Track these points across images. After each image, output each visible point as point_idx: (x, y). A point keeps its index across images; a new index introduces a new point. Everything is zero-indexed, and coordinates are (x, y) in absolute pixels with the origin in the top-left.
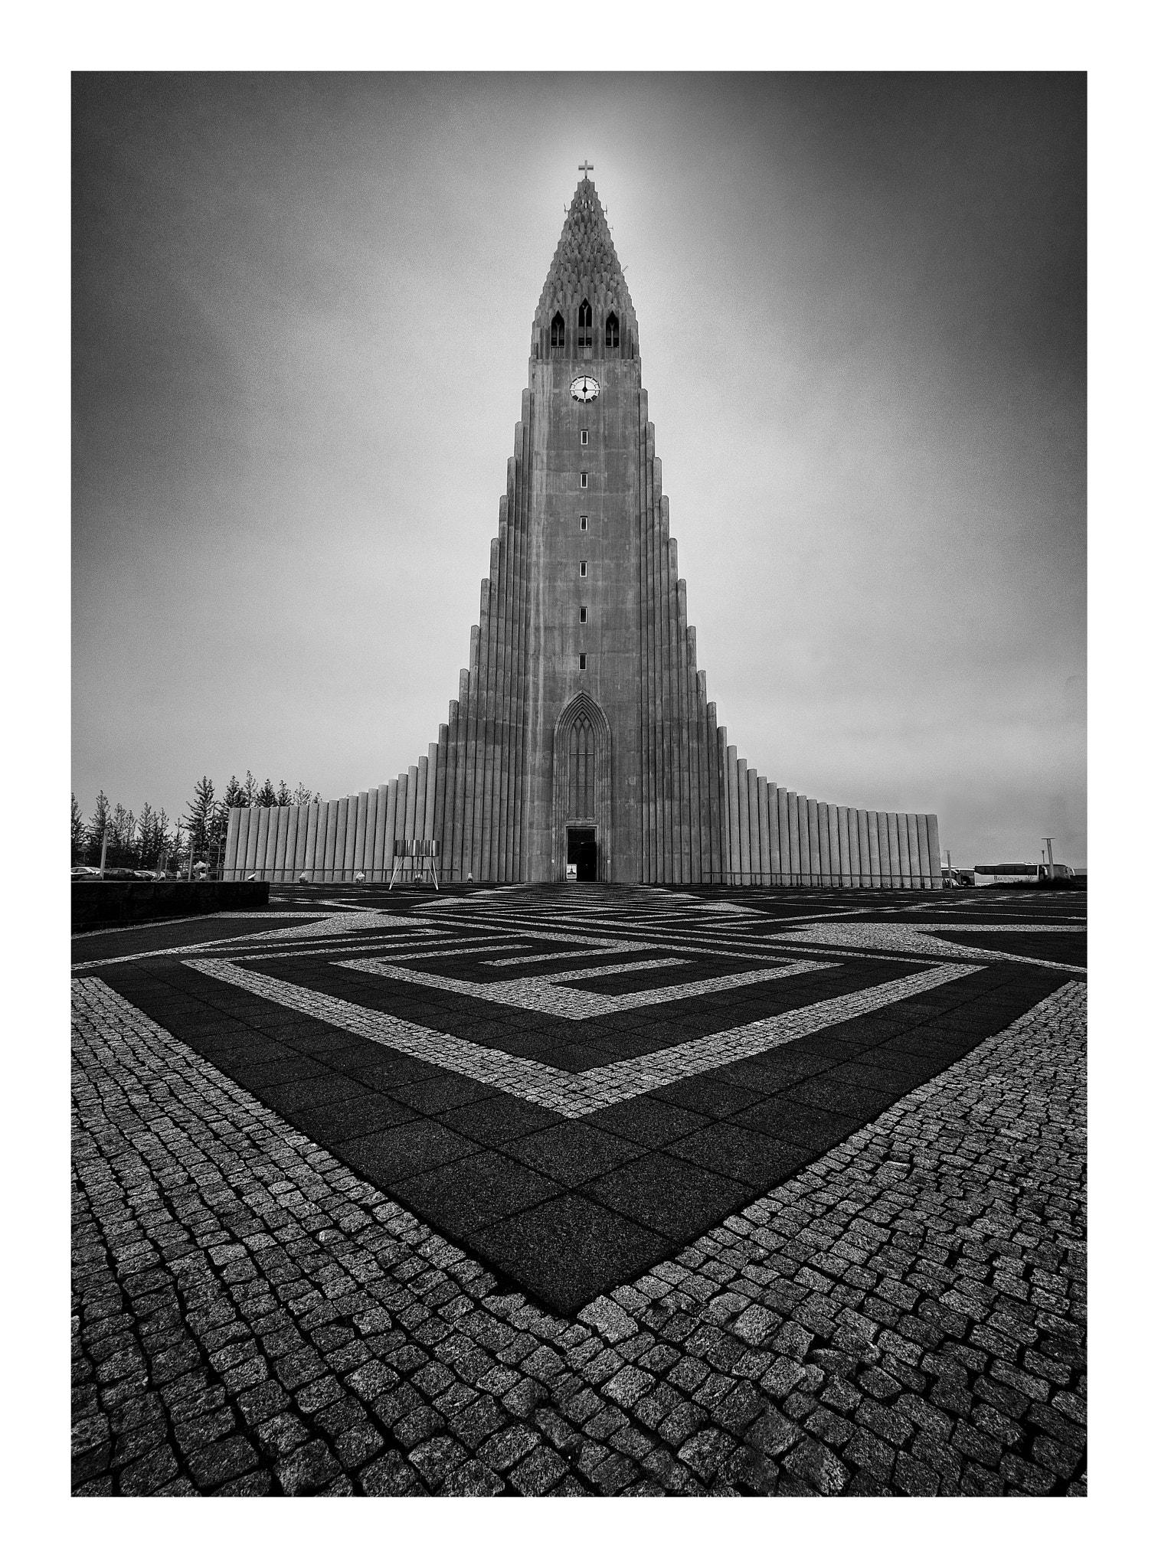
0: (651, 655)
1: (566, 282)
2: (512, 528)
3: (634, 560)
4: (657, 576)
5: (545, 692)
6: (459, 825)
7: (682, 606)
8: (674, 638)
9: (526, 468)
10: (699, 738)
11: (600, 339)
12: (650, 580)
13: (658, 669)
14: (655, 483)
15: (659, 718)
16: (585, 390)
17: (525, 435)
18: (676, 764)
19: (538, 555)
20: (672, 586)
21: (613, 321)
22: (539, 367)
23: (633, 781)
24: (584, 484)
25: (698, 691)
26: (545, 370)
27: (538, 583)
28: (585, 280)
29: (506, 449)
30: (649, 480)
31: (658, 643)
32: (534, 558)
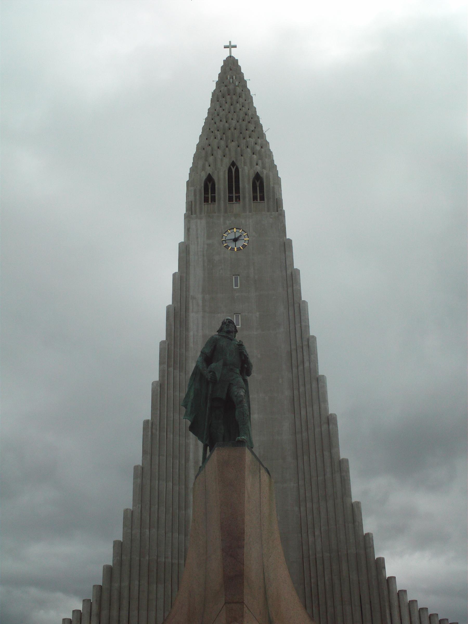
1: (215, 147)
2: (171, 369)
8: (328, 470)
11: (247, 195)
12: (303, 413)
14: (303, 324)
16: (235, 240)
25: (354, 522)
28: (233, 145)
30: (297, 320)
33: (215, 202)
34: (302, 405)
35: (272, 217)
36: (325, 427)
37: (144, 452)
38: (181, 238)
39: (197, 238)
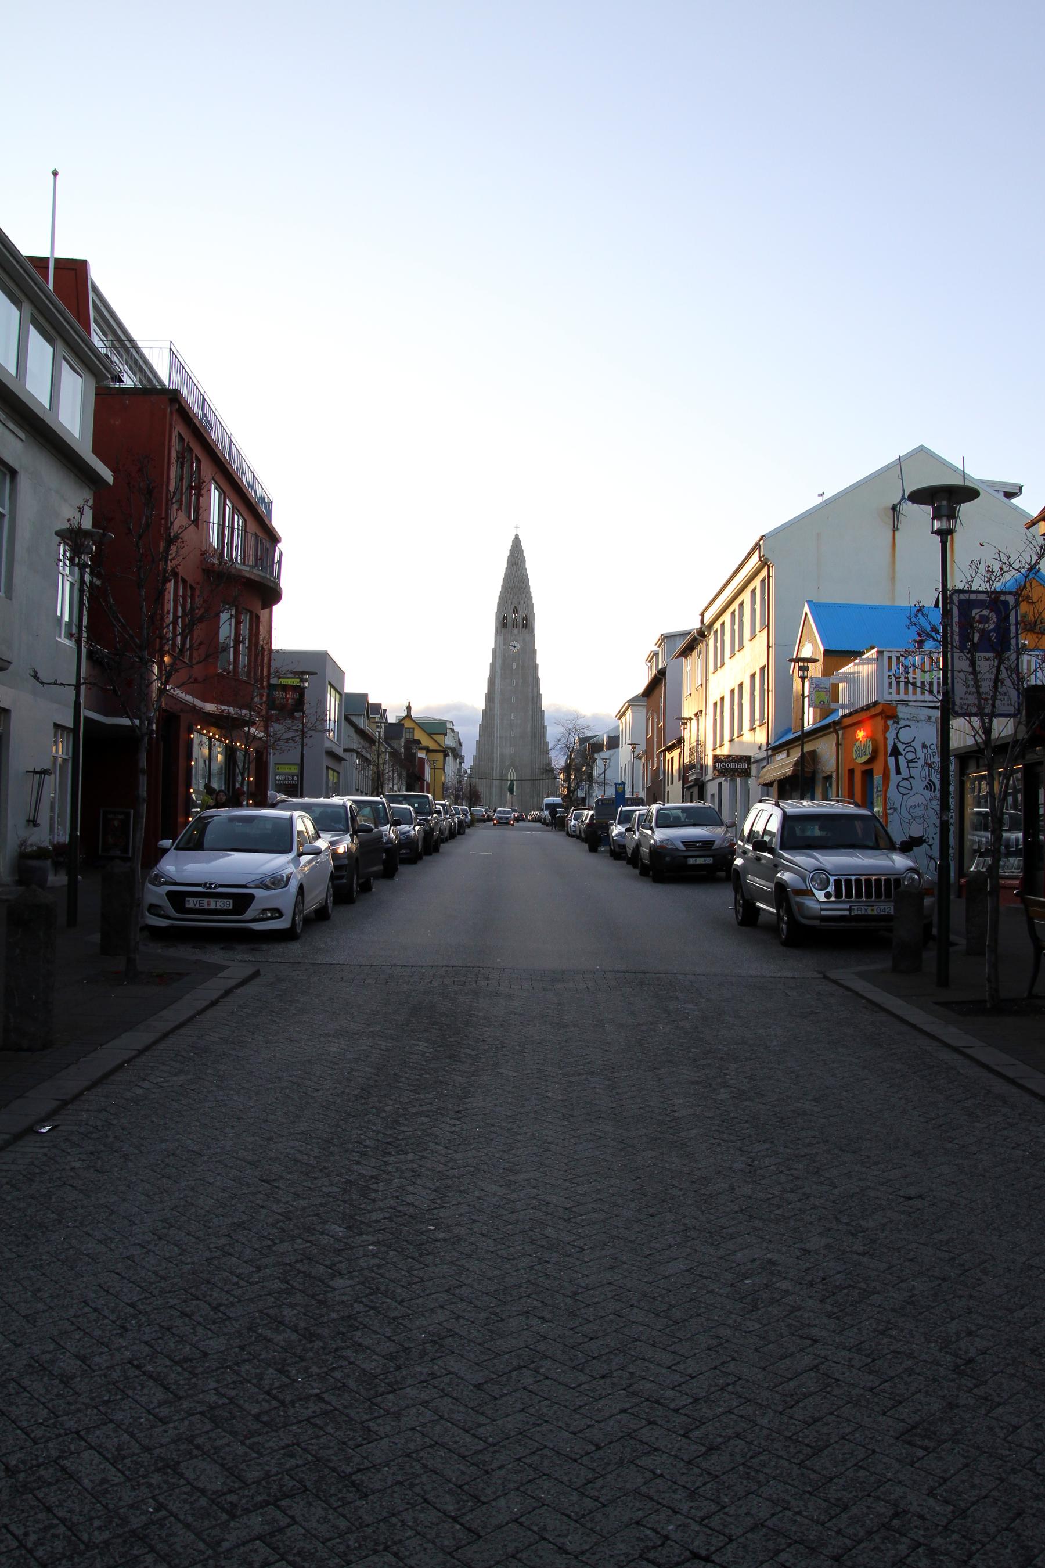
3: (530, 713)
17: (493, 666)
21: (525, 618)
23: (529, 790)
27: (497, 721)
29: (487, 673)
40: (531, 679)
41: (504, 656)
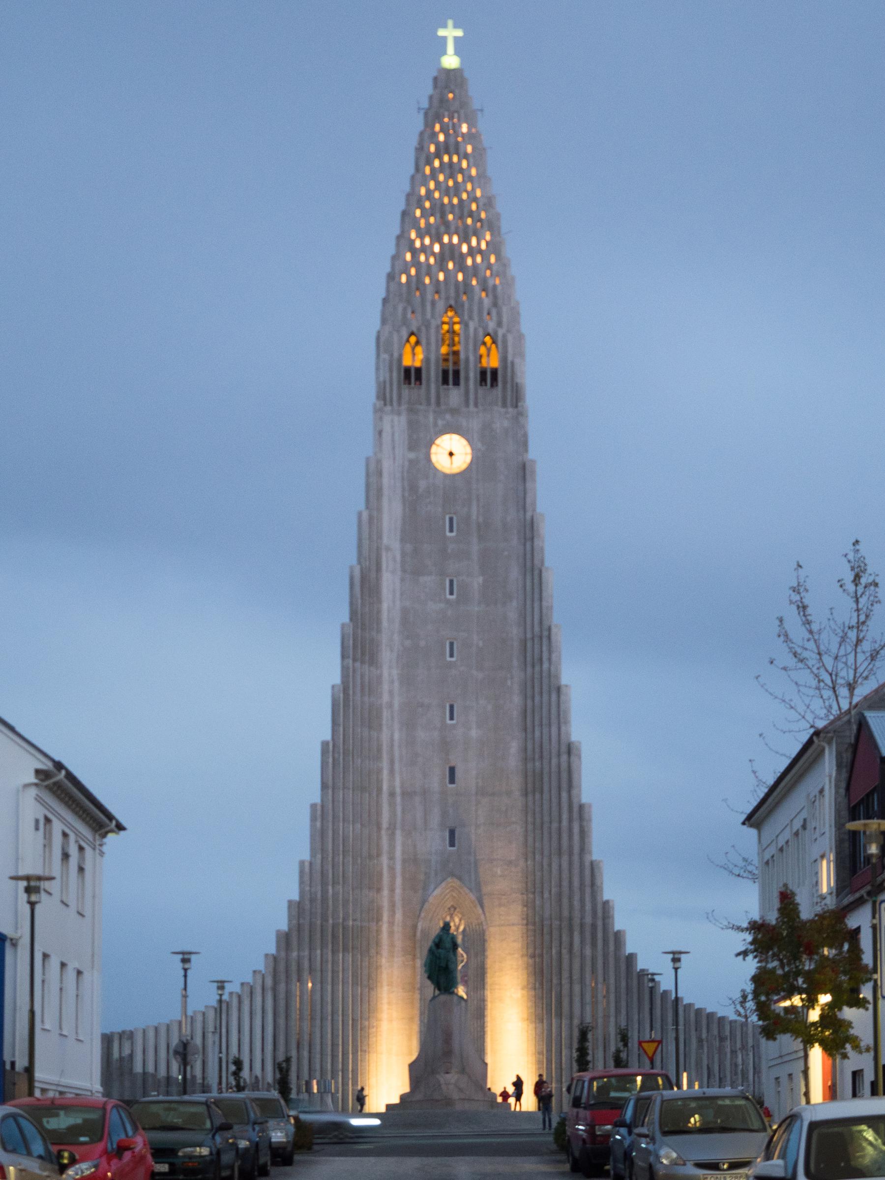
0: (538, 832)
2: (358, 664)
3: (517, 699)
4: (545, 731)
5: (404, 879)
6: (305, 1054)
7: (575, 776)
8: (565, 816)
9: (373, 575)
10: (594, 945)
11: (472, 375)
12: (537, 734)
13: (546, 852)
14: (544, 604)
15: (547, 914)
18: (565, 974)
19: (391, 693)
20: (564, 749)
22: (387, 419)
24: (451, 593)
25: (593, 884)
26: (396, 423)
30: (536, 596)
31: (546, 819)
32: (386, 698)
33: (421, 384)
34: (537, 723)
35: (508, 416)
36: (564, 758)
37: (324, 786)
38: (369, 450)
39: (394, 448)
40: (515, 573)
41: (413, 487)
